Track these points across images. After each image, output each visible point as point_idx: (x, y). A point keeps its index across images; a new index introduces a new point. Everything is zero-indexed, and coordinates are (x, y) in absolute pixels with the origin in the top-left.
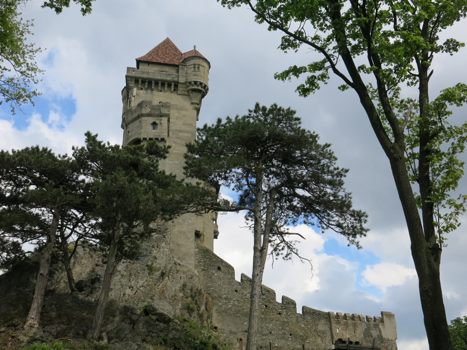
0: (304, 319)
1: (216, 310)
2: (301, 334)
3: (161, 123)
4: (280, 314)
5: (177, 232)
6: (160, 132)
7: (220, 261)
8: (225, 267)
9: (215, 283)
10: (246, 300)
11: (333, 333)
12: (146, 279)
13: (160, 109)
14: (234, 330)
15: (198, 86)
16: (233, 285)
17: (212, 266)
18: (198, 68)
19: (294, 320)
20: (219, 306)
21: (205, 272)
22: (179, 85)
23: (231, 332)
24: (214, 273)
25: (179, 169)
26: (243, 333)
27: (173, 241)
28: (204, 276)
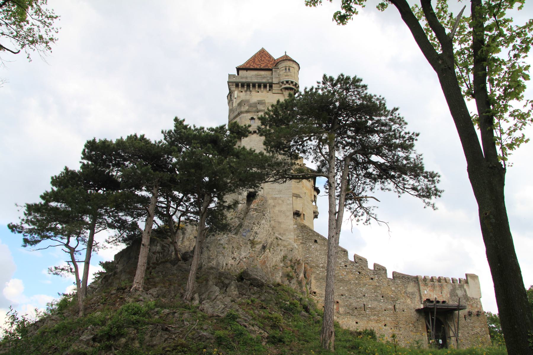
0: (394, 282)
1: (315, 278)
2: (392, 296)
4: (372, 279)
10: (341, 268)
11: (422, 294)
12: (249, 251)
13: (257, 106)
18: (289, 69)
19: (385, 284)
20: (317, 273)
22: (273, 86)
26: (340, 297)
28: (303, 249)
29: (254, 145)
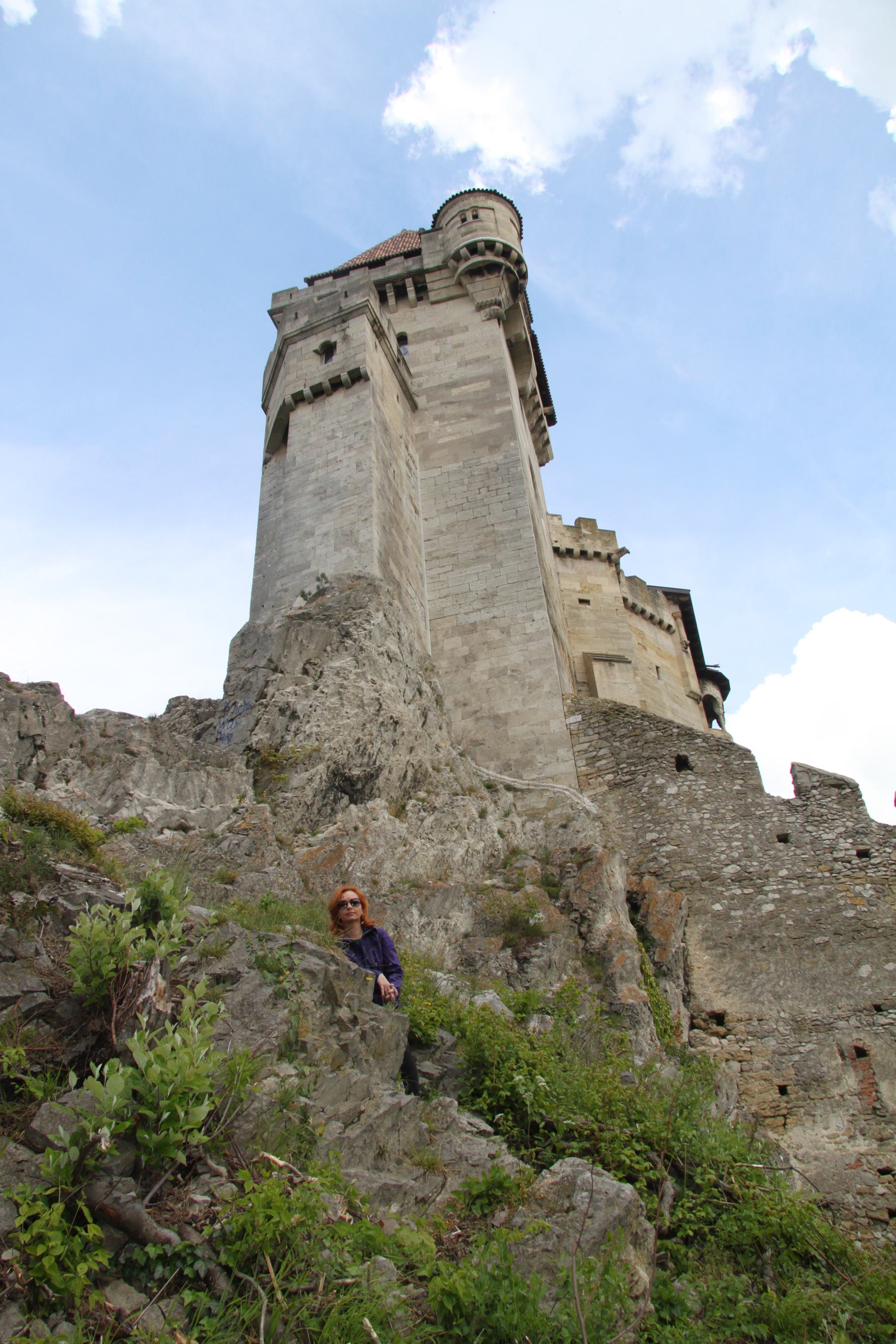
1: (704, 939)
3: (346, 338)
5: (485, 677)
6: (345, 359)
7: (679, 734)
8: (710, 751)
9: (677, 825)
10: (838, 866)
12: (235, 803)
14: (811, 1012)
15: (483, 254)
16: (761, 817)
17: (648, 759)
20: (716, 915)
21: (621, 790)
22: (428, 278)
23: (799, 1025)
24: (662, 787)
25: (463, 484)
26: (865, 1019)
27: (476, 712)
28: (622, 809)
29: (336, 426)
